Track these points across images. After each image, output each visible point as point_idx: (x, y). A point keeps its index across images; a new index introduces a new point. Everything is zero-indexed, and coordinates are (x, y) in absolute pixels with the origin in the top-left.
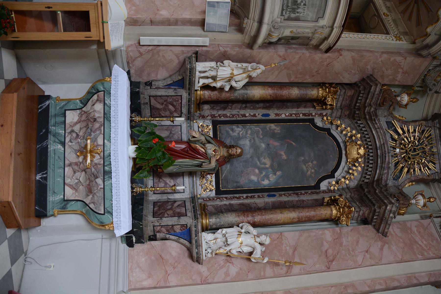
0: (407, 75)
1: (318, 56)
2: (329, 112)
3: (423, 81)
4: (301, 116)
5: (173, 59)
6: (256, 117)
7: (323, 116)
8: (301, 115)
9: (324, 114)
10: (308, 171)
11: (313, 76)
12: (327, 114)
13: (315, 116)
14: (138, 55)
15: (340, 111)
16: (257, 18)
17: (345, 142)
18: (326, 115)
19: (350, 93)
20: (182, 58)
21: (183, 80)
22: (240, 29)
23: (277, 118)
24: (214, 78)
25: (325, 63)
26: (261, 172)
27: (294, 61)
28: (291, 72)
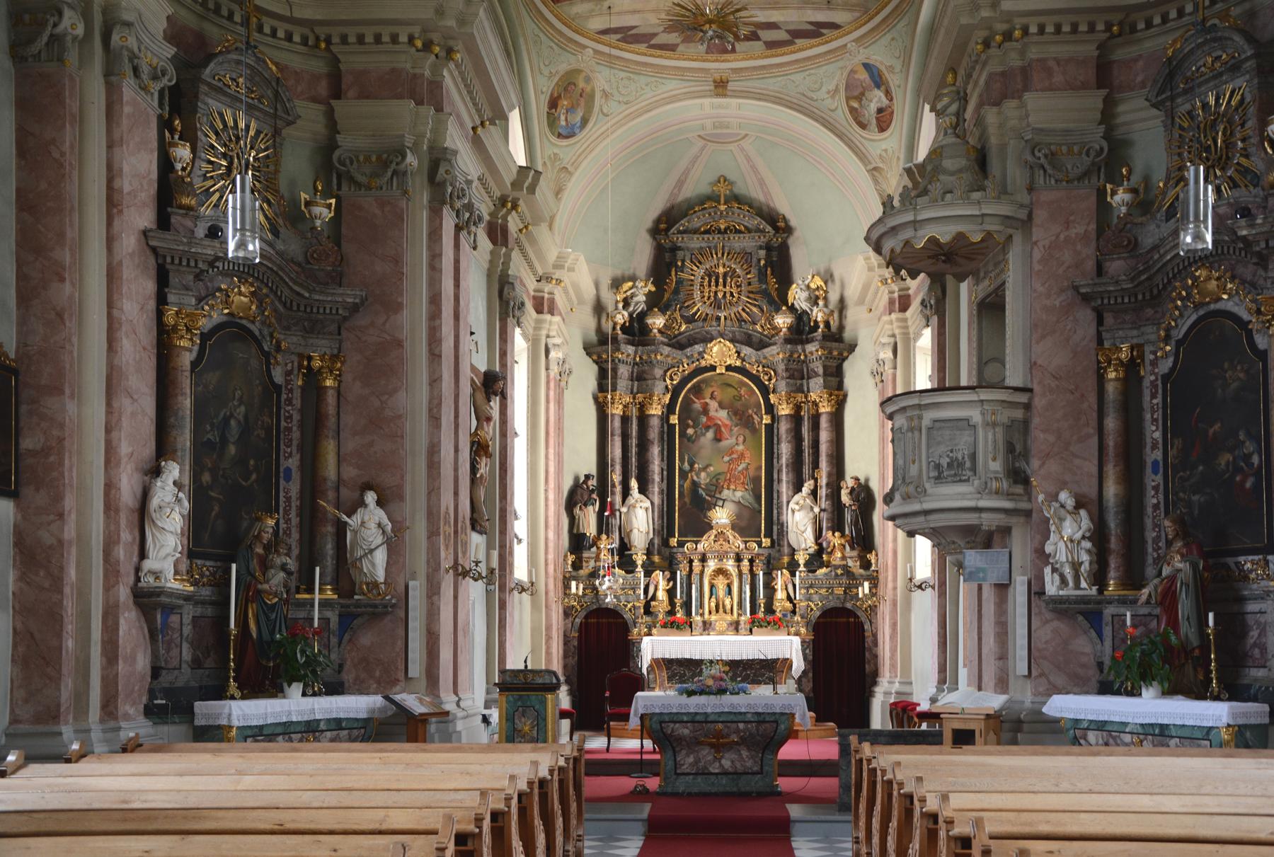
0: (1072, 218)
1: (1039, 402)
2: (1148, 349)
3: (1079, 179)
4: (1158, 400)
5: (1049, 630)
6: (1158, 485)
7: (1157, 358)
8: (1155, 401)
9: (1152, 357)
10: (1239, 379)
11: (1083, 395)
12: (1151, 352)
13: (1156, 374)
14: (1043, 680)
15: (1143, 329)
16: (977, 515)
17: (1197, 306)
18: (1155, 353)
19: (1109, 319)
20: (1048, 615)
21: (1086, 615)
22: (1006, 531)
23: (1160, 446)
24: (1076, 566)
25: (1054, 384)
26: (1241, 470)
27: (1052, 438)
28: (1075, 438)
